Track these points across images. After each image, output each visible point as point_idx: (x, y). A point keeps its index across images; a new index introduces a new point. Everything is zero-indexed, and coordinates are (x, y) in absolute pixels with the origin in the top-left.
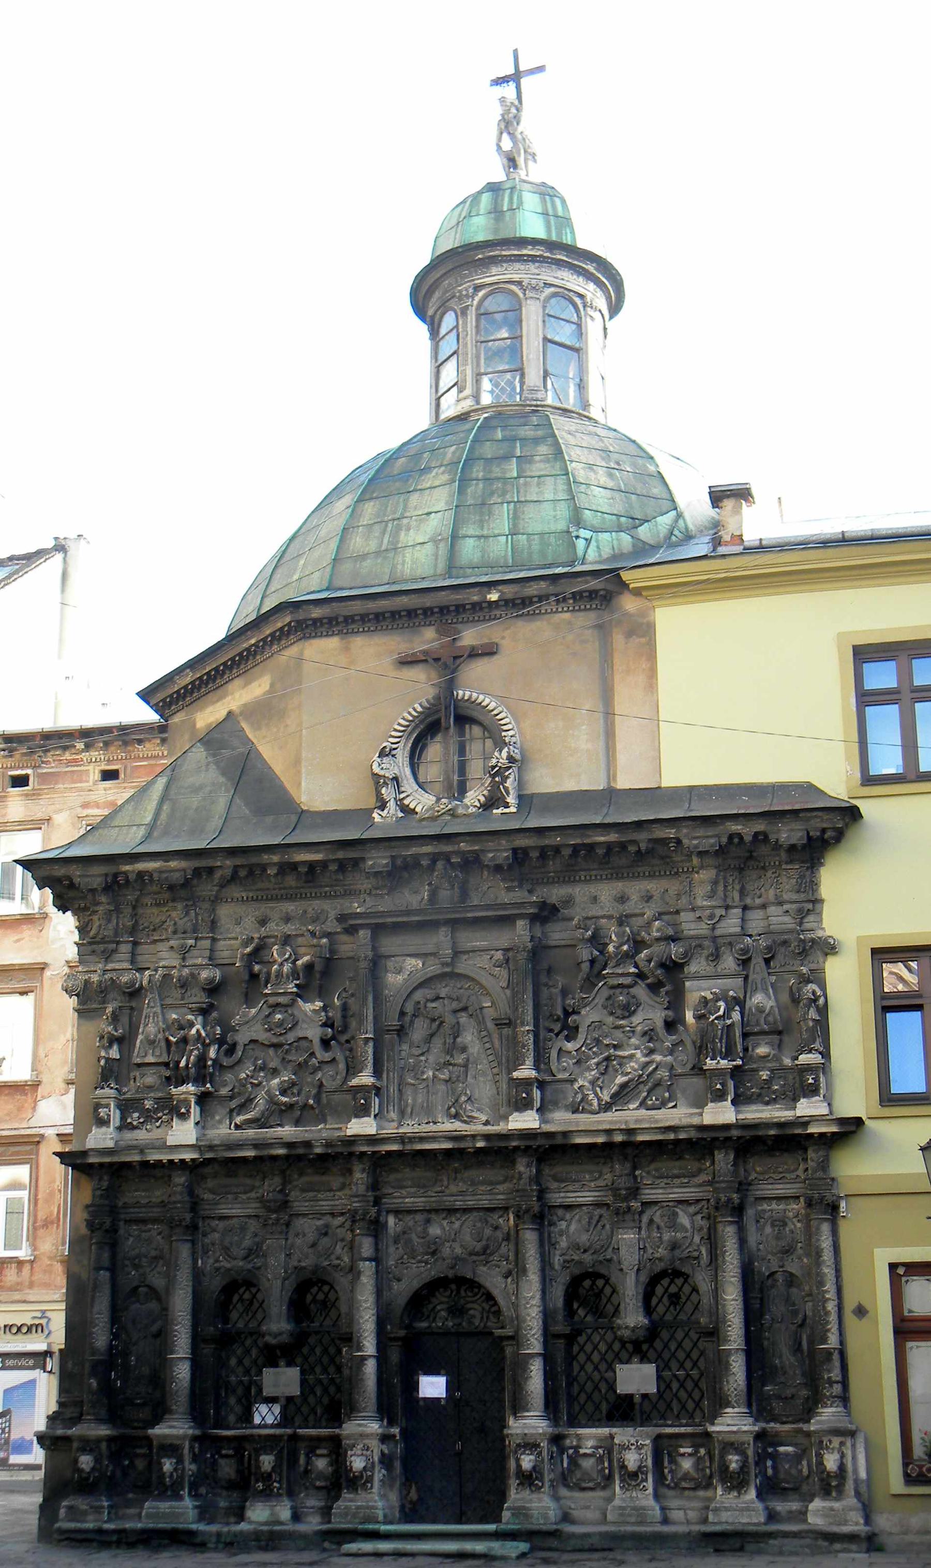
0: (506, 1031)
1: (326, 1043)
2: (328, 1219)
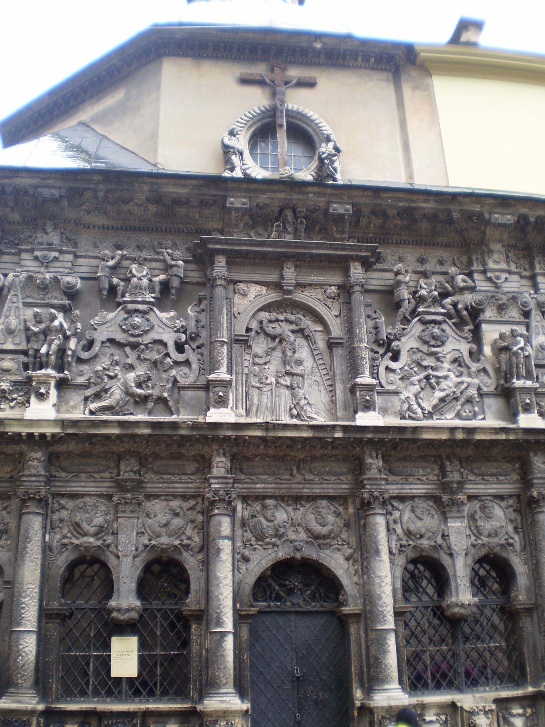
1: (180, 348)
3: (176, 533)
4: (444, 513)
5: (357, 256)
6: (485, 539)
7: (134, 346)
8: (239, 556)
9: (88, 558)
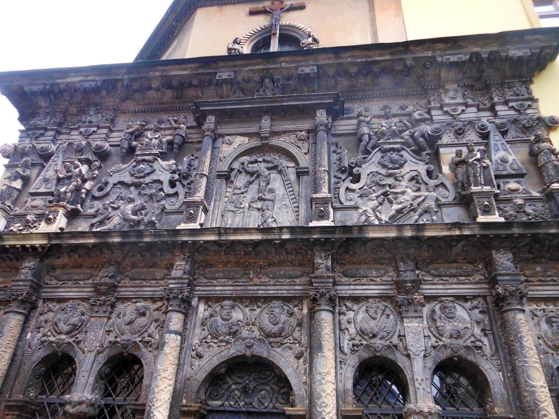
0: (305, 178)
1: (172, 184)
2: (148, 304)
3: (139, 331)
4: (400, 313)
5: (322, 103)
6: (446, 340)
7: (137, 186)
8: (193, 353)
9: (59, 353)
